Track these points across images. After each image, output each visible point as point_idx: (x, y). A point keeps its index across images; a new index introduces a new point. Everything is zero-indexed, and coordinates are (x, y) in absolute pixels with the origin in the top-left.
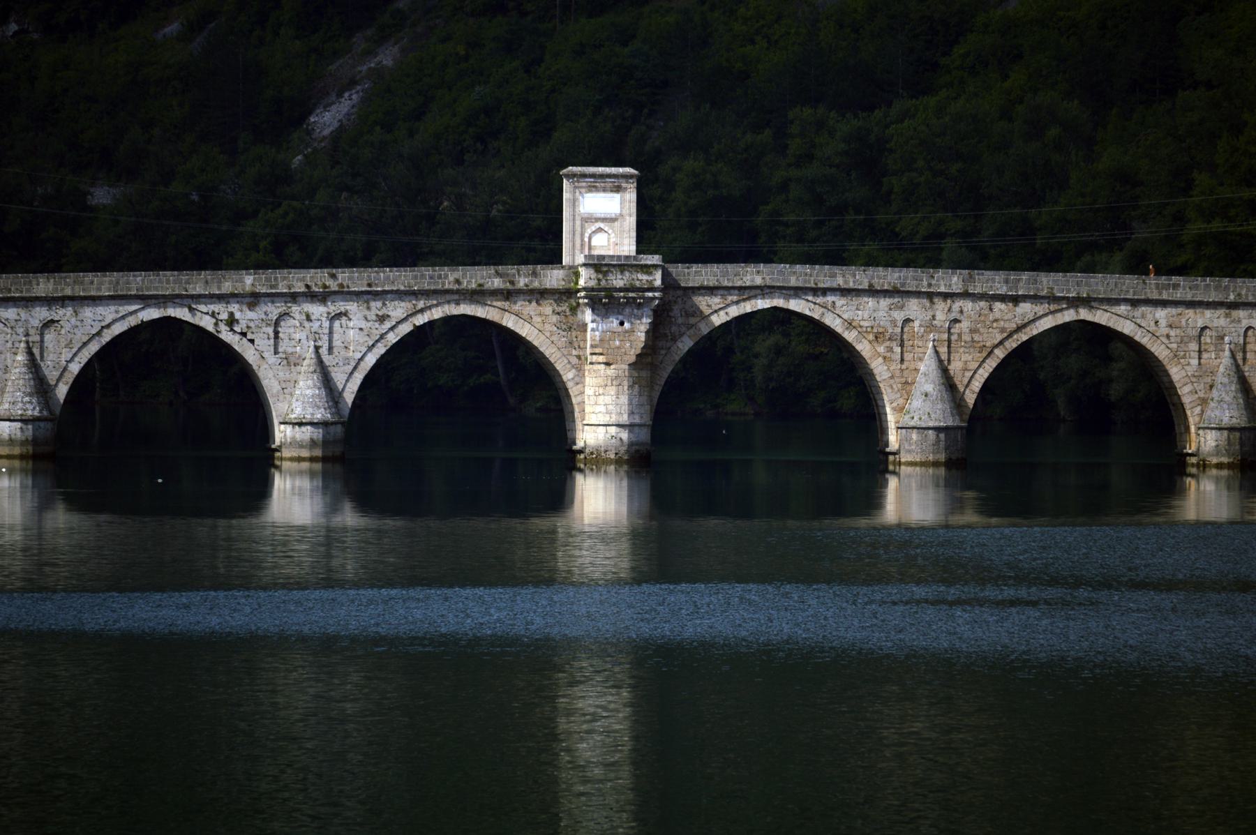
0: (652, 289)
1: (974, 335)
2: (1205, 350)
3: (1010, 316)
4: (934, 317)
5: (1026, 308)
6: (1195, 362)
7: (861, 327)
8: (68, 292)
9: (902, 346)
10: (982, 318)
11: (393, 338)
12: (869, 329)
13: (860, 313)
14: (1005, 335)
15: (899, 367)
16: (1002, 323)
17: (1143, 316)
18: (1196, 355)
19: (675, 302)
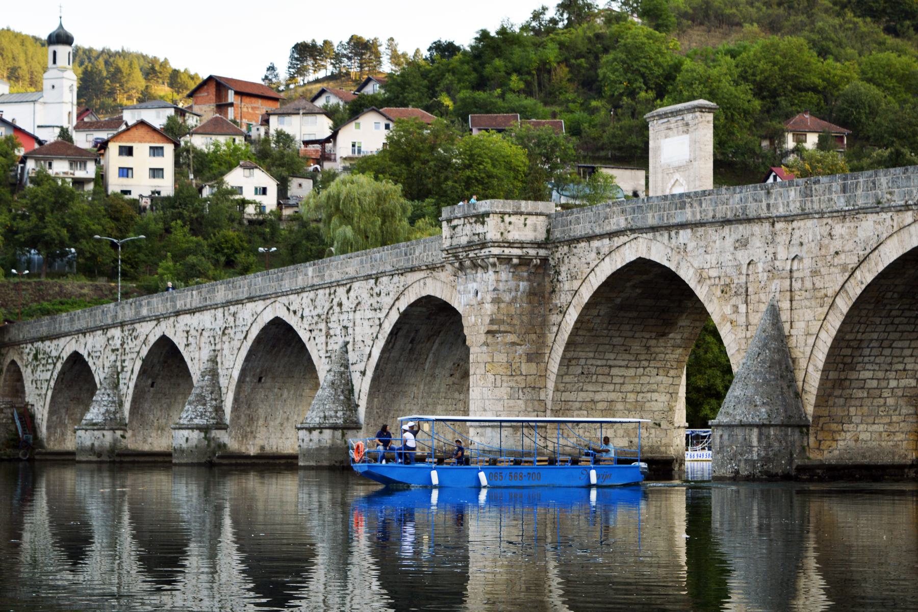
0: (483, 245)
3: (849, 246)
5: (868, 226)
7: (710, 278)
9: (746, 303)
10: (823, 252)
11: (388, 327)
13: (708, 257)
14: (847, 275)
15: (744, 335)
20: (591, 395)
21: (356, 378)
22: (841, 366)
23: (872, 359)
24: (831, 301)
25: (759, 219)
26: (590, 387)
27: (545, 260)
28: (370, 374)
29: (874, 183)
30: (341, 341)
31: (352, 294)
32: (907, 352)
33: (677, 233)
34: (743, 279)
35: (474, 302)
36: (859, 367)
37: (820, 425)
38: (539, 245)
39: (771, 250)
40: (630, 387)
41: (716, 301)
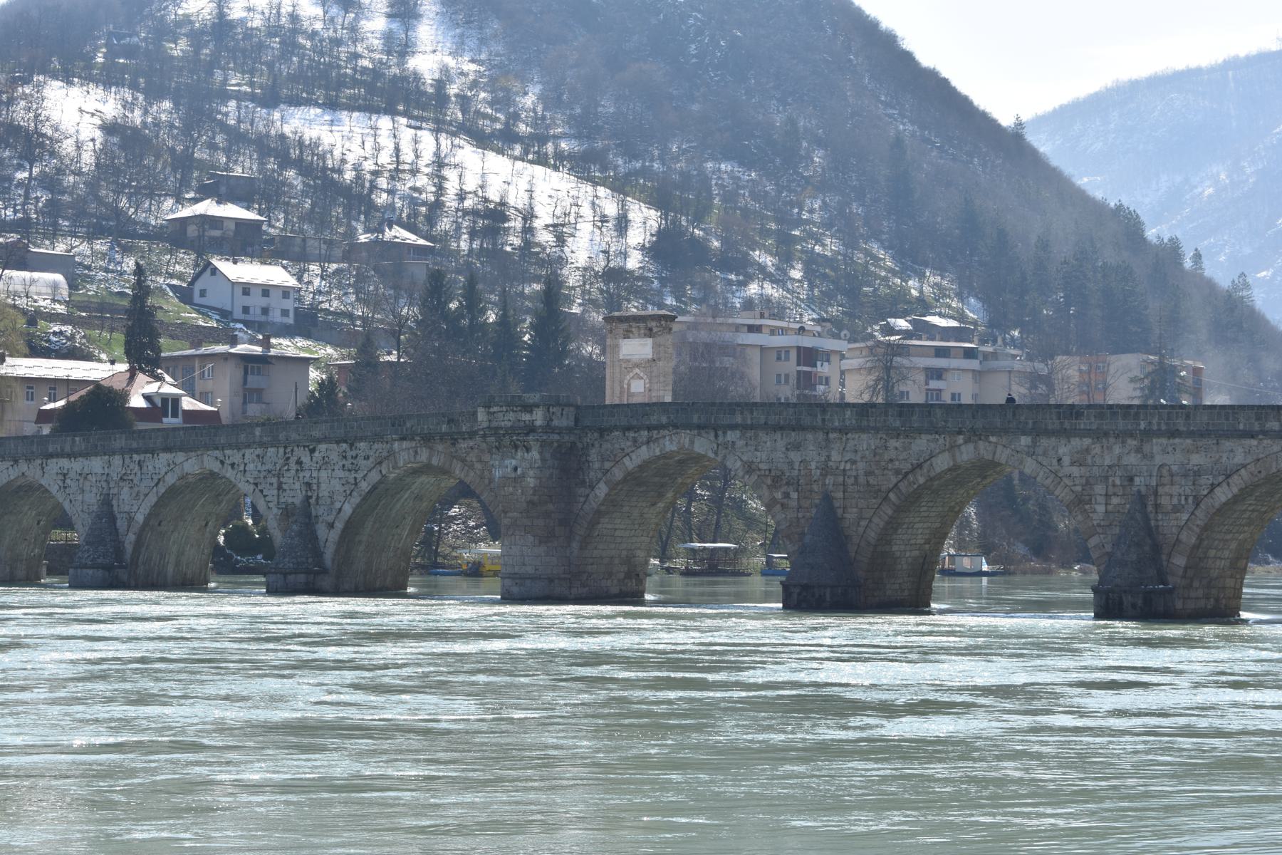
1: (869, 478)
2: (1115, 494)
3: (903, 455)
4: (828, 457)
5: (922, 444)
6: (1101, 509)
7: (760, 470)
8: (135, 445)
10: (877, 458)
11: (365, 486)
12: (767, 473)
13: (758, 454)
14: (900, 477)
16: (897, 463)
17: (1045, 454)
18: (1101, 499)
19: (593, 445)
21: (321, 531)
25: (814, 429)
27: (574, 443)
28: (339, 525)
31: (316, 454)
33: (725, 433)
34: (796, 473)
38: (570, 430)
39: (824, 453)
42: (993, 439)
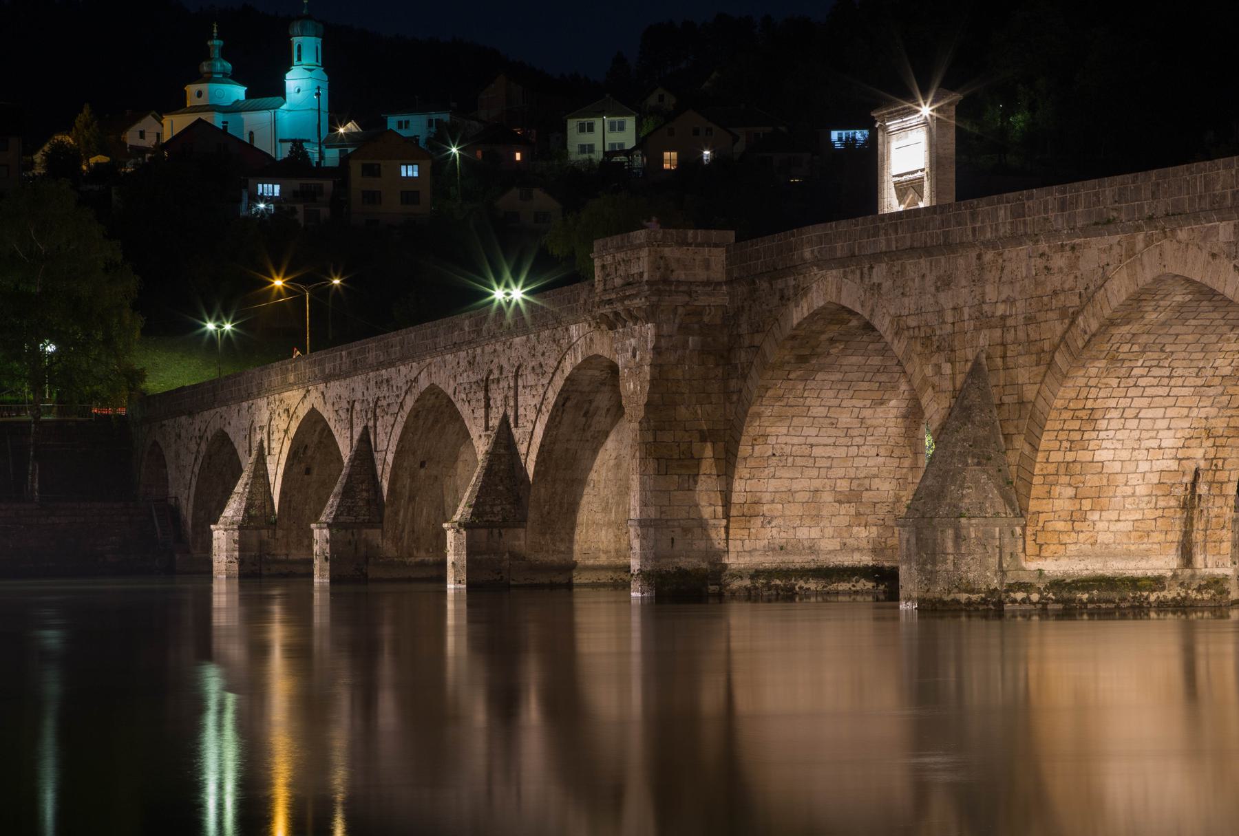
4: (983, 295)
7: (908, 328)
11: (552, 397)
13: (906, 300)
20: (787, 483)
22: (1066, 444)
23: (1111, 433)
24: (1047, 357)
26: (785, 473)
29: (1097, 195)
30: (501, 411)
32: (1164, 424)
33: (871, 268)
35: (632, 364)
36: (1092, 445)
37: (1041, 524)
40: (841, 473)
41: (916, 359)
42: (1182, 235)
